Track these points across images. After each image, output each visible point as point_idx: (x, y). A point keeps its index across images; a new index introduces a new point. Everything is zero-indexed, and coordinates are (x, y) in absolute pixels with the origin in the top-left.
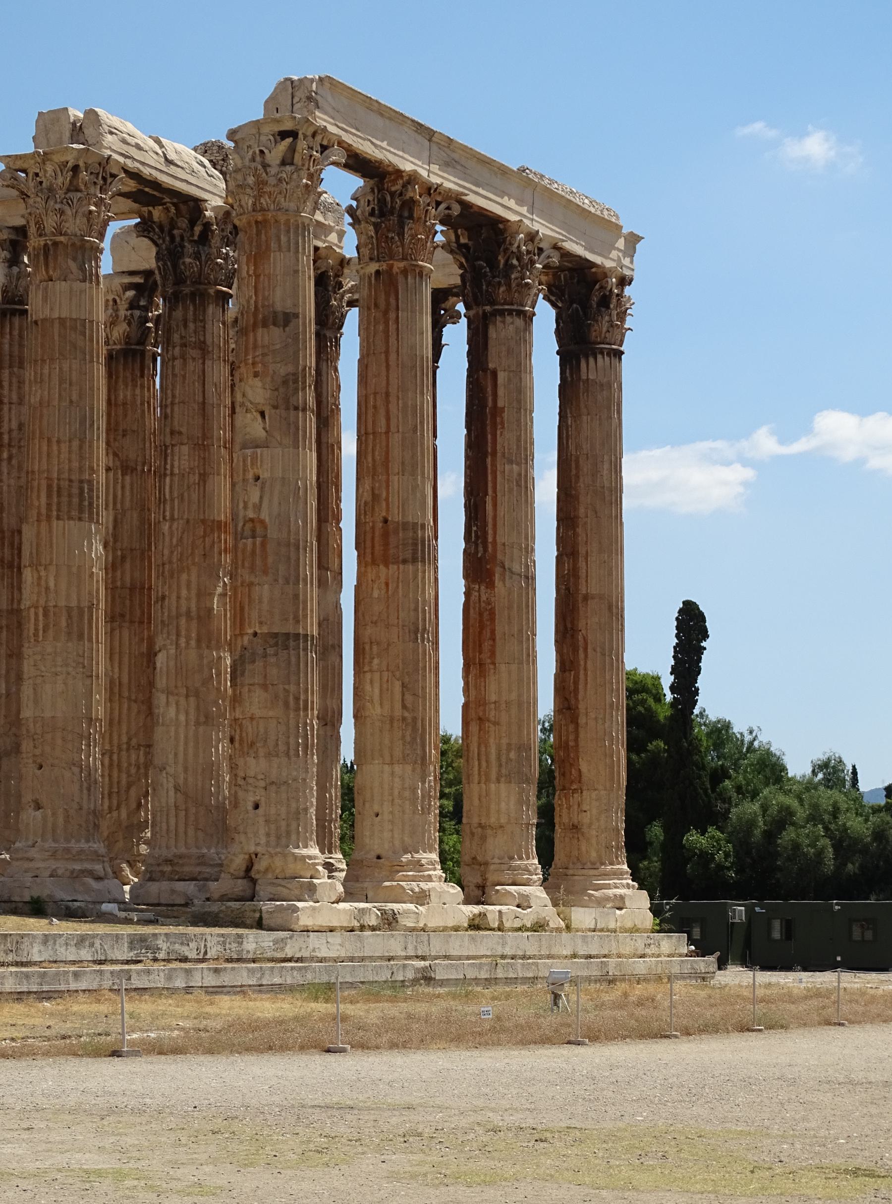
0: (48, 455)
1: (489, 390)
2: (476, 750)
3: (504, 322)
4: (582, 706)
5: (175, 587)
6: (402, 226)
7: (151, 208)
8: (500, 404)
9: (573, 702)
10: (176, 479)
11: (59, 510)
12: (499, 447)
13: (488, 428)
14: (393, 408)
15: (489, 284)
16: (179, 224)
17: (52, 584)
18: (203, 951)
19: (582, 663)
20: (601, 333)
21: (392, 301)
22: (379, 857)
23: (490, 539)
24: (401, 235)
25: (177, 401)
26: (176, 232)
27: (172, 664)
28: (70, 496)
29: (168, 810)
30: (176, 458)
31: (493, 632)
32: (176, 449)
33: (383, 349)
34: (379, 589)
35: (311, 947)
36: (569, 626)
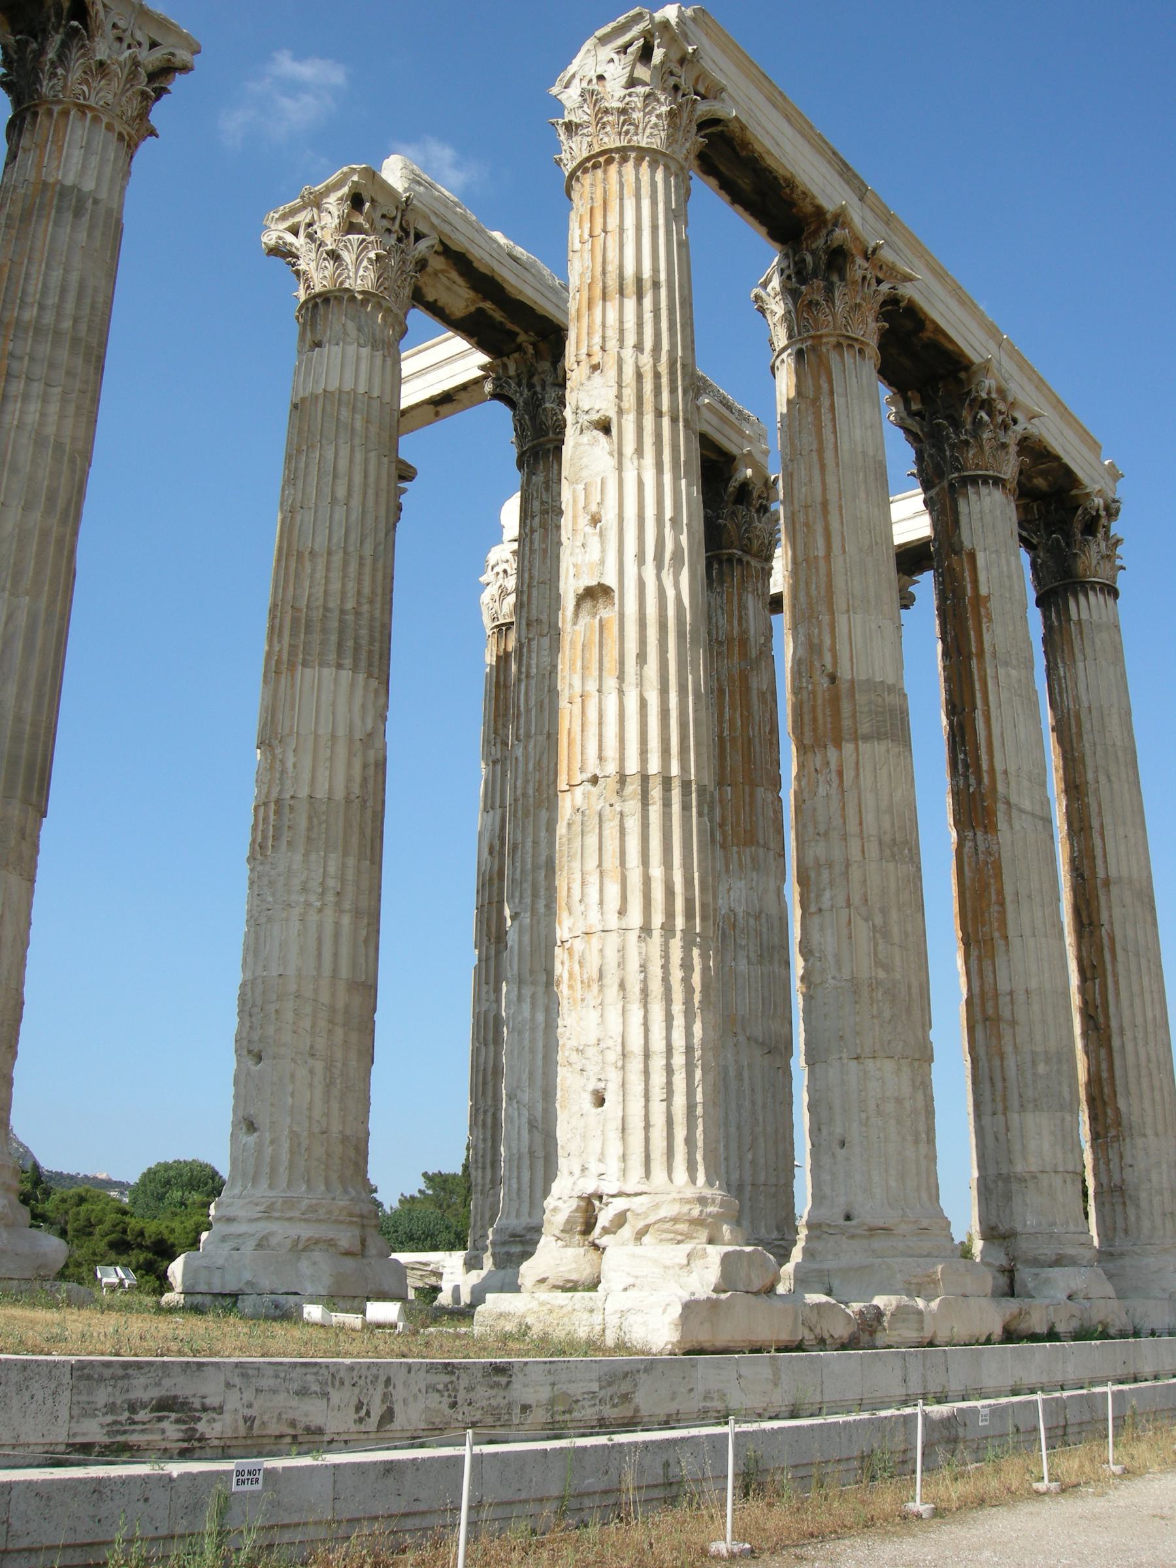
0: (297, 576)
1: (967, 574)
2: (986, 1065)
3: (978, 493)
4: (1114, 1023)
5: (530, 830)
6: (829, 290)
7: (505, 359)
8: (983, 591)
9: (1101, 1020)
10: (533, 682)
11: (306, 652)
12: (987, 646)
13: (970, 622)
14: (835, 525)
15: (953, 447)
16: (540, 370)
17: (289, 764)
18: (377, 1411)
19: (1109, 967)
20: (1089, 567)
21: (825, 387)
22: (848, 1218)
23: (985, 766)
24: (830, 299)
25: (535, 583)
26: (535, 380)
27: (526, 939)
28: (324, 631)
29: (519, 1158)
30: (534, 655)
31: (1000, 892)
32: (534, 644)
33: (815, 447)
34: (829, 783)
35: (700, 1389)
36: (1086, 921)
